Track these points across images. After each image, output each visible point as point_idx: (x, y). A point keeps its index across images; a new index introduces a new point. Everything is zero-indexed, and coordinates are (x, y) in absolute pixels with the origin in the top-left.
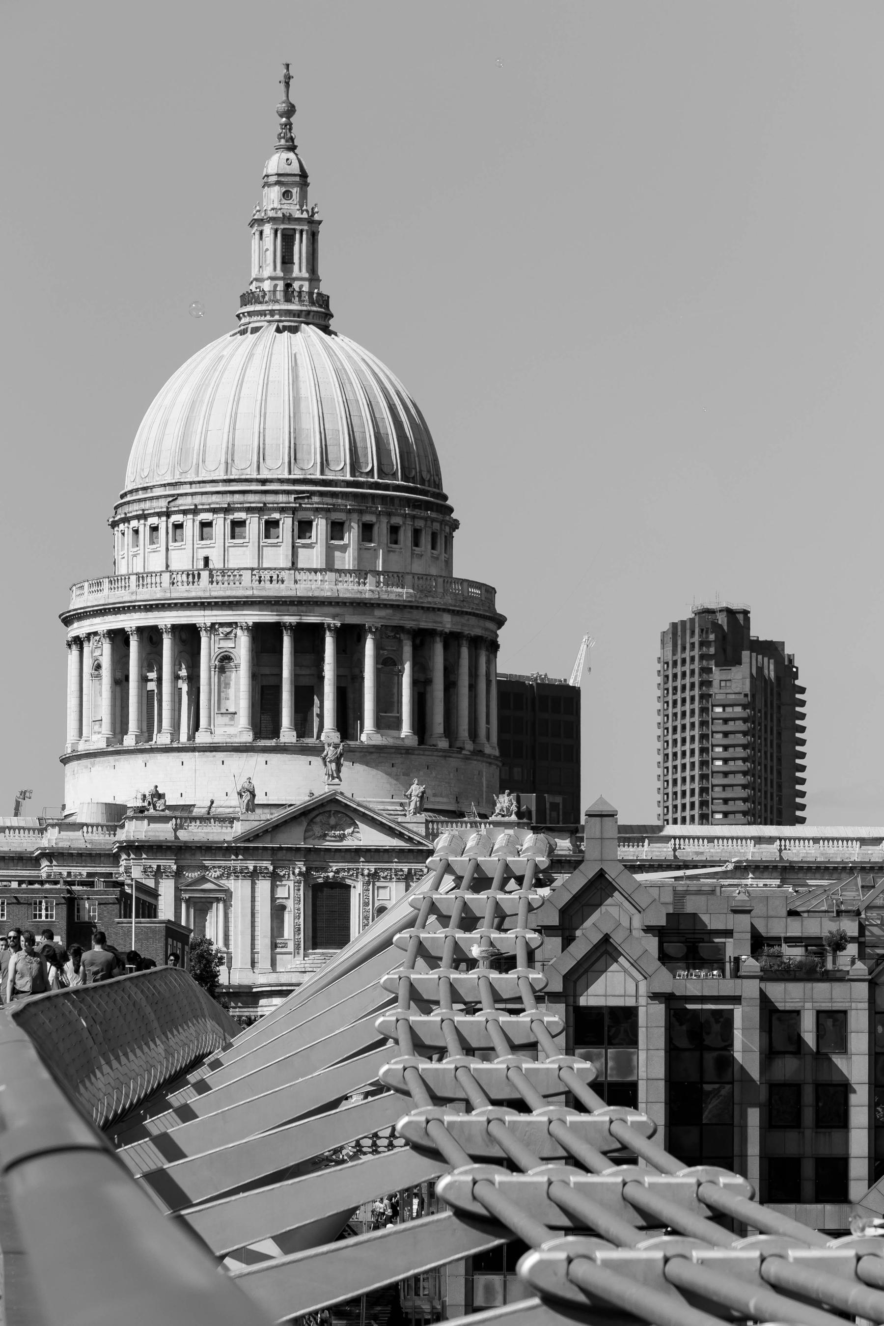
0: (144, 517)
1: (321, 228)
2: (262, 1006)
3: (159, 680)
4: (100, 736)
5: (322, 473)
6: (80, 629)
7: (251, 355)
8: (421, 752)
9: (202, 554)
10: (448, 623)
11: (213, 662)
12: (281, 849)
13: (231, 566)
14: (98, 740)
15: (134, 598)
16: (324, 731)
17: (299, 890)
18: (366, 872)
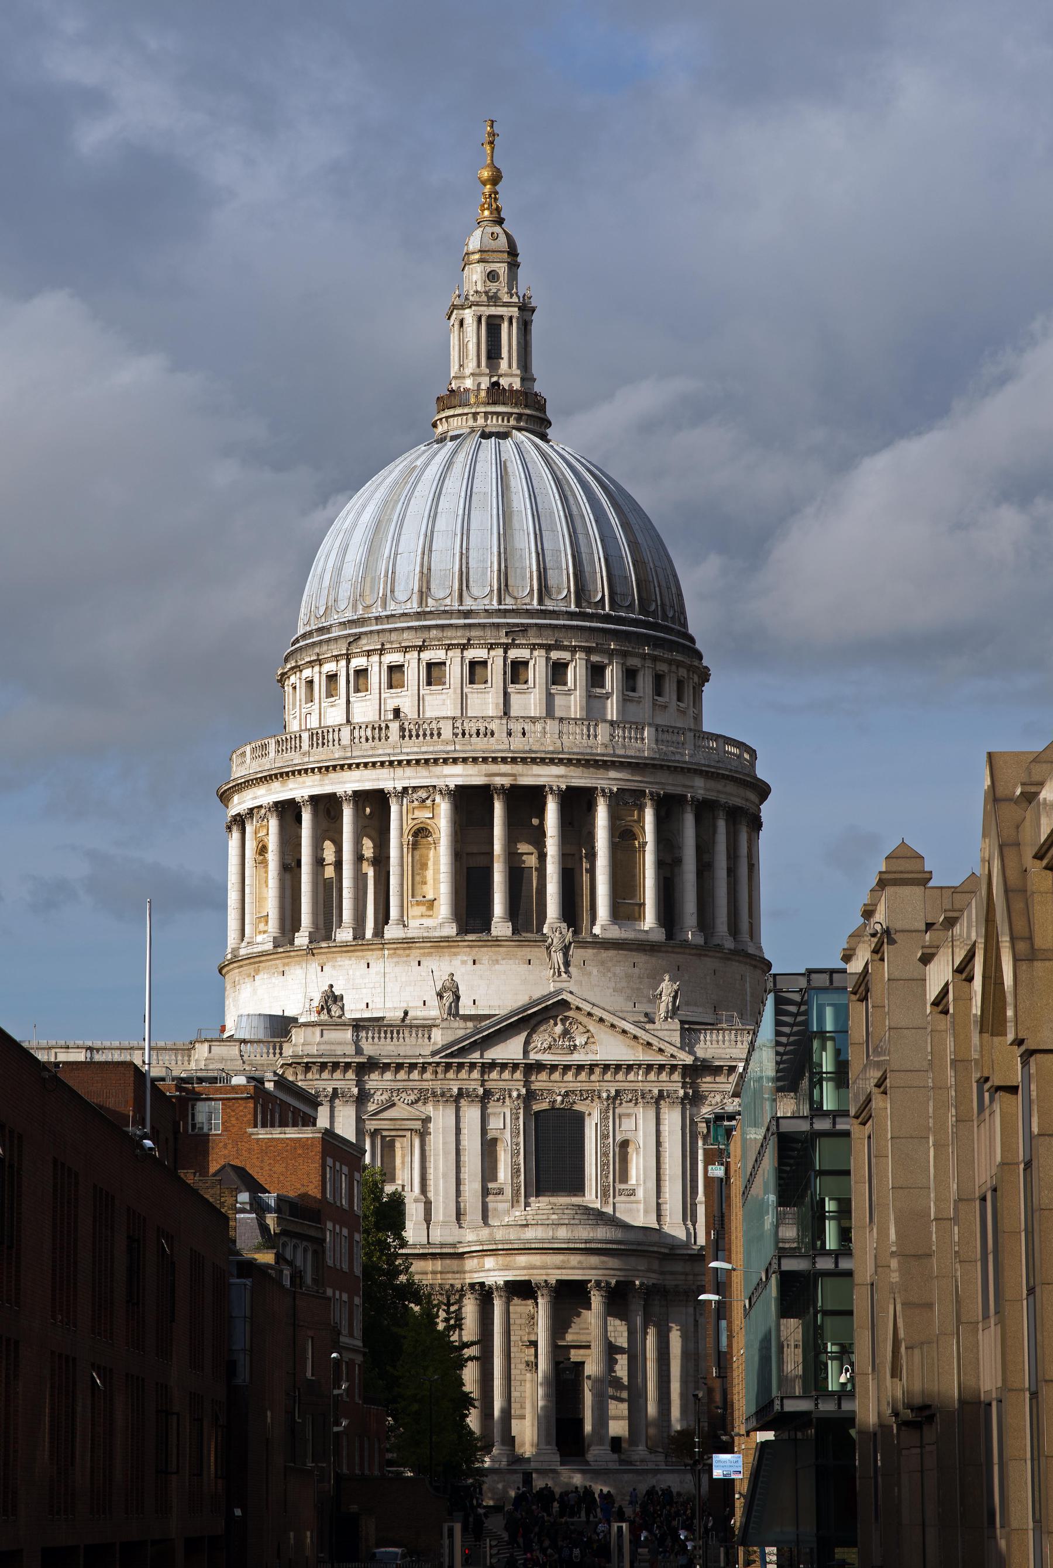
0: (320, 662)
1: (535, 317)
2: (471, 1272)
3: (338, 865)
4: (265, 936)
5: (541, 601)
6: (240, 804)
7: (449, 464)
8: (670, 949)
9: (391, 705)
10: (699, 788)
11: (405, 836)
12: (492, 1065)
13: (428, 715)
14: (264, 941)
15: (306, 759)
16: (548, 921)
17: (518, 1118)
18: (604, 1095)
